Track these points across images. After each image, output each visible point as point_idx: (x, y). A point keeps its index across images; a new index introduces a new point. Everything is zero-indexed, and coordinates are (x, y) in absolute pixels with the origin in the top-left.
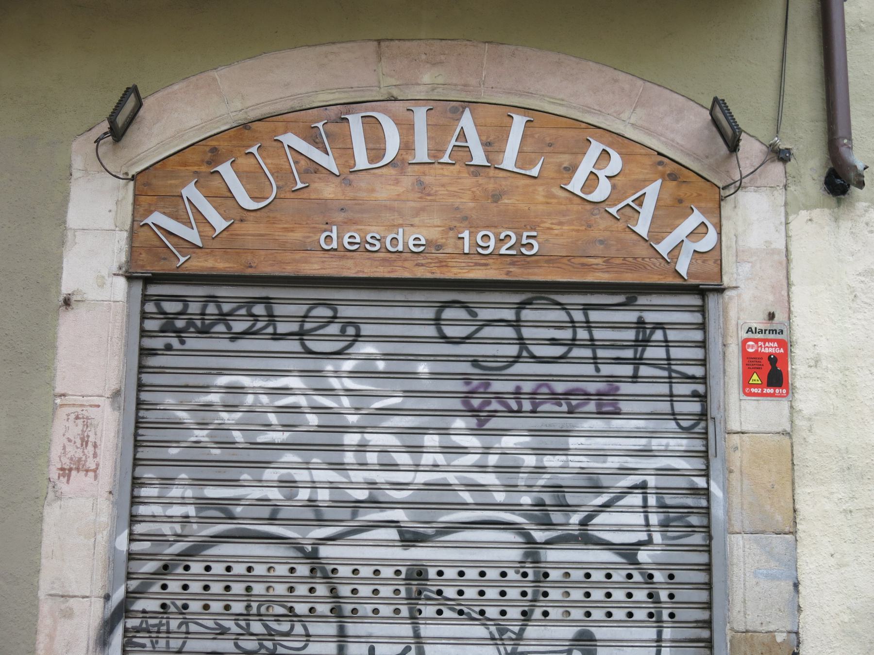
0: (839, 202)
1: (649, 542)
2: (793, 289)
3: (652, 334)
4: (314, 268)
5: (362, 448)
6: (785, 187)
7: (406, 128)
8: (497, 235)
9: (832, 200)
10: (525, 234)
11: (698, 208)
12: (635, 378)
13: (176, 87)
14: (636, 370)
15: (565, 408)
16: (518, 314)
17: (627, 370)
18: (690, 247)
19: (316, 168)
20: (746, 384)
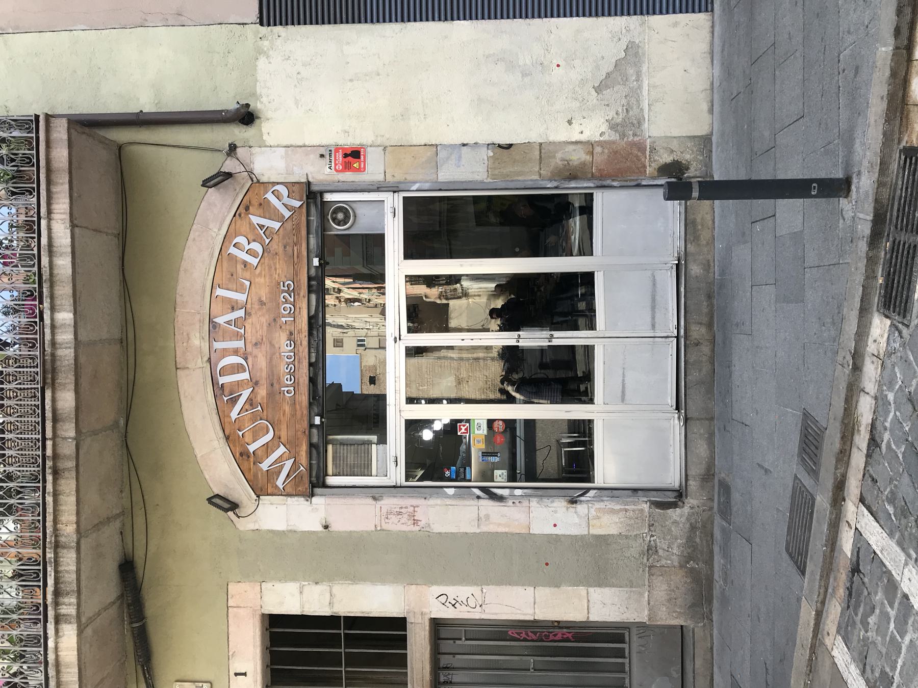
0: (258, 118)
2: (307, 144)
6: (250, 147)
7: (225, 353)
9: (257, 122)
10: (282, 288)
18: (286, 200)
19: (250, 402)
20: (359, 170)
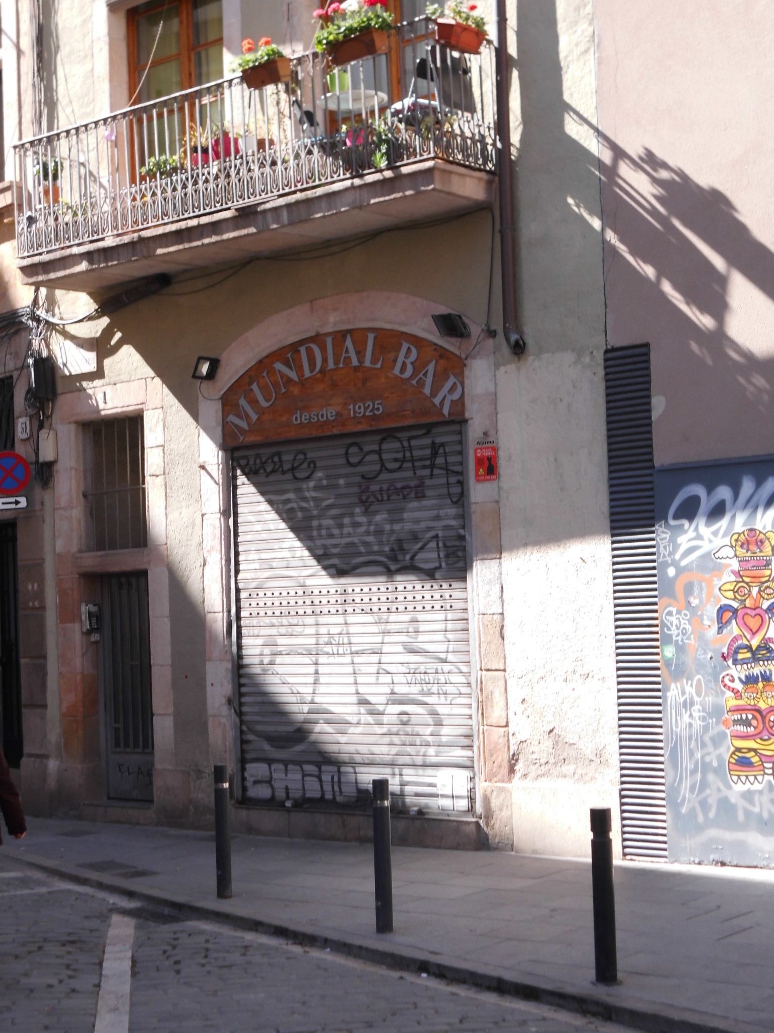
0: (519, 359)
1: (440, 567)
2: (499, 416)
3: (438, 450)
4: (292, 435)
5: (320, 527)
6: (494, 353)
7: (323, 350)
8: (364, 405)
9: (516, 358)
10: (376, 403)
11: (453, 374)
12: (432, 476)
13: (233, 345)
14: (432, 472)
15: (401, 496)
16: (380, 447)
17: (427, 472)
18: (449, 398)
20: (477, 475)
